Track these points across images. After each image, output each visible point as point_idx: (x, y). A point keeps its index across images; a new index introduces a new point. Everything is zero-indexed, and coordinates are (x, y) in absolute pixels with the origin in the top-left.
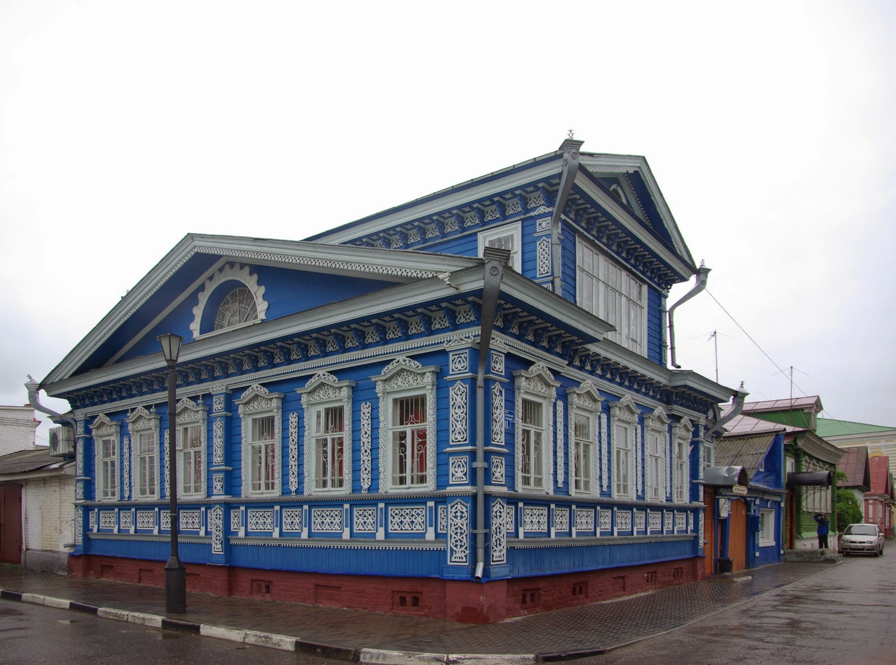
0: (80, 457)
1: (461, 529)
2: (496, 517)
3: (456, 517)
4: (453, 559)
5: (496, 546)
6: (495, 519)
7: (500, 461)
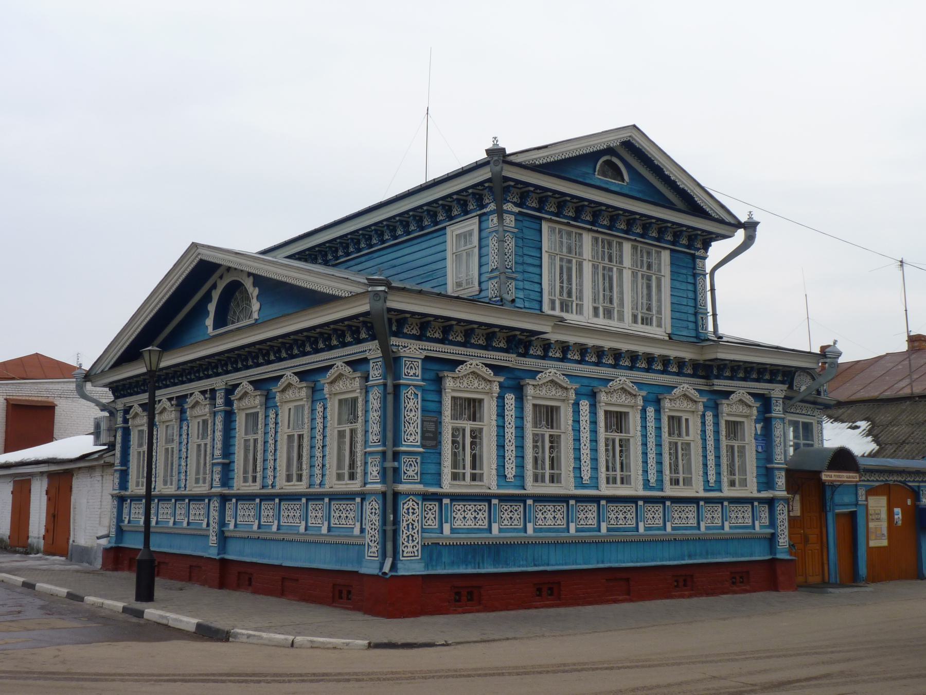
0: (118, 447)
2: (408, 513)
4: (369, 555)
5: (408, 542)
6: (406, 515)
7: (414, 460)
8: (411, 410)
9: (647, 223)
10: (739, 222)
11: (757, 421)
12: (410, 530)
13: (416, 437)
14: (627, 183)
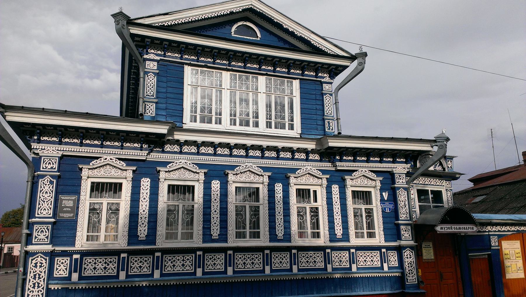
2: (36, 266)
6: (34, 268)
7: (45, 228)
9: (275, 62)
10: (352, 55)
11: (382, 190)
13: (50, 211)
14: (260, 38)
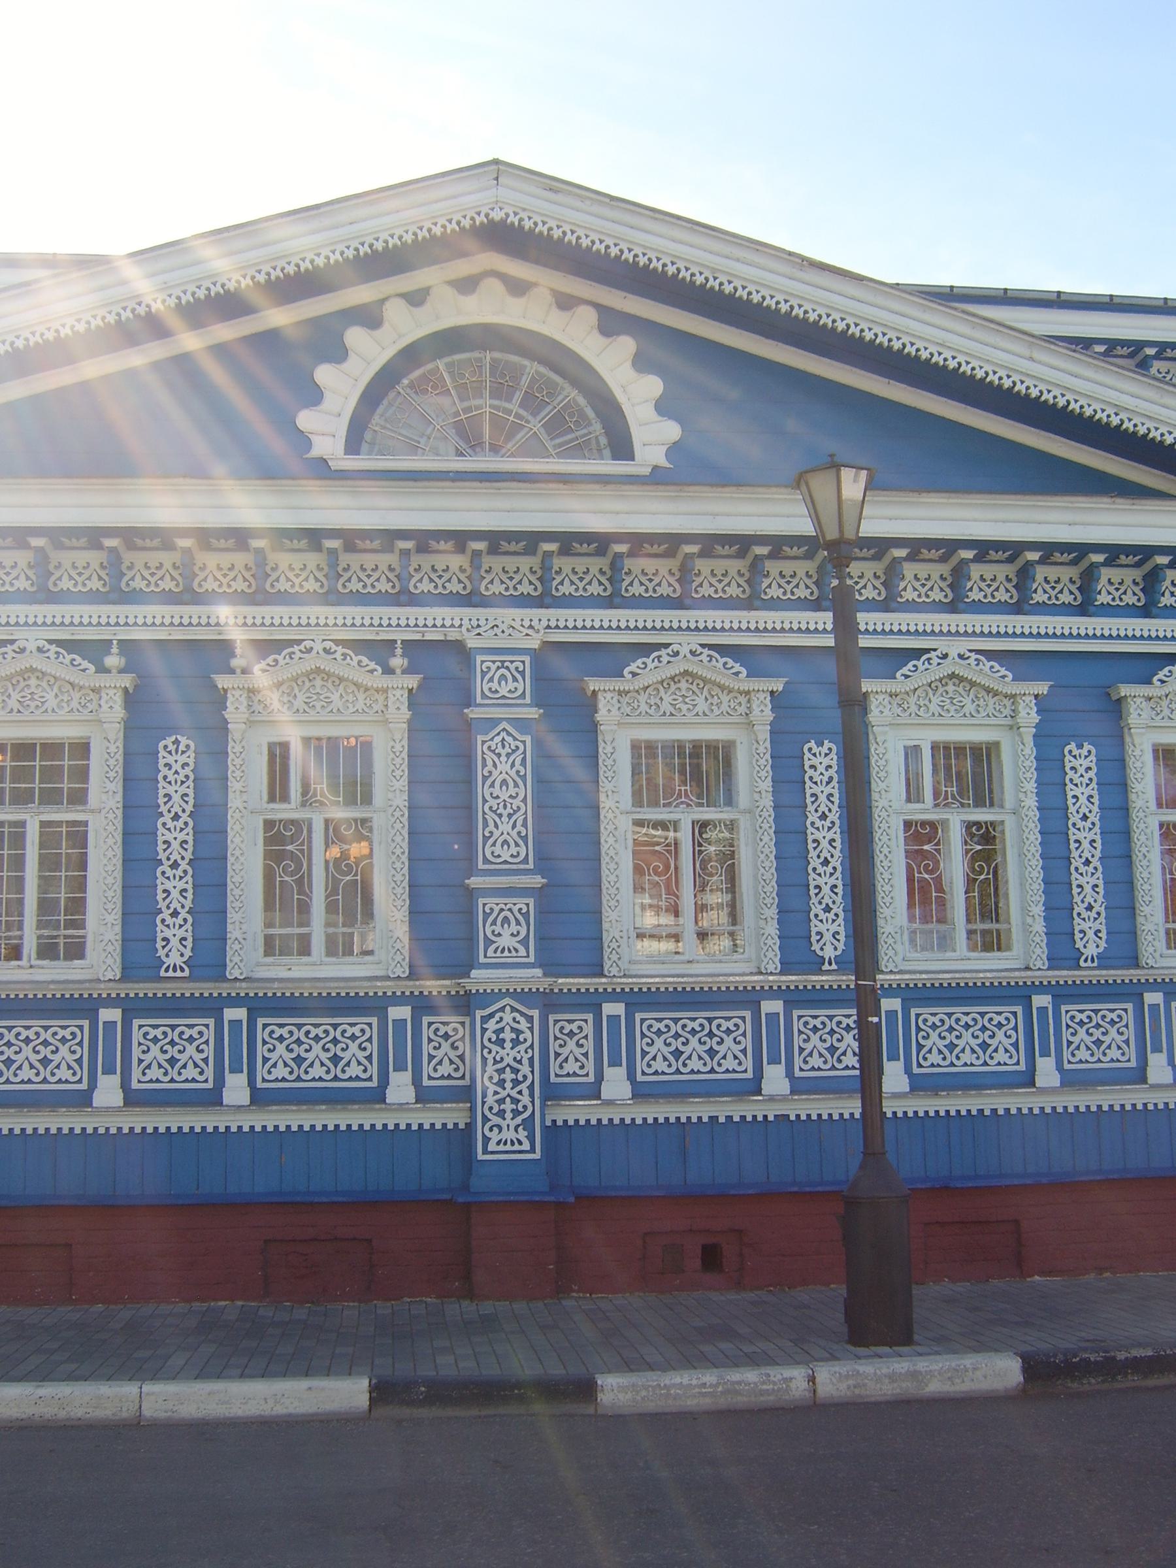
1: (516, 1071)
3: (500, 1043)
8: (504, 782)
12: (508, 1085)
